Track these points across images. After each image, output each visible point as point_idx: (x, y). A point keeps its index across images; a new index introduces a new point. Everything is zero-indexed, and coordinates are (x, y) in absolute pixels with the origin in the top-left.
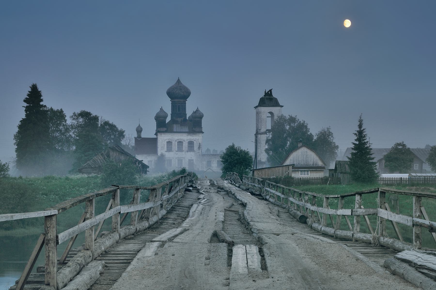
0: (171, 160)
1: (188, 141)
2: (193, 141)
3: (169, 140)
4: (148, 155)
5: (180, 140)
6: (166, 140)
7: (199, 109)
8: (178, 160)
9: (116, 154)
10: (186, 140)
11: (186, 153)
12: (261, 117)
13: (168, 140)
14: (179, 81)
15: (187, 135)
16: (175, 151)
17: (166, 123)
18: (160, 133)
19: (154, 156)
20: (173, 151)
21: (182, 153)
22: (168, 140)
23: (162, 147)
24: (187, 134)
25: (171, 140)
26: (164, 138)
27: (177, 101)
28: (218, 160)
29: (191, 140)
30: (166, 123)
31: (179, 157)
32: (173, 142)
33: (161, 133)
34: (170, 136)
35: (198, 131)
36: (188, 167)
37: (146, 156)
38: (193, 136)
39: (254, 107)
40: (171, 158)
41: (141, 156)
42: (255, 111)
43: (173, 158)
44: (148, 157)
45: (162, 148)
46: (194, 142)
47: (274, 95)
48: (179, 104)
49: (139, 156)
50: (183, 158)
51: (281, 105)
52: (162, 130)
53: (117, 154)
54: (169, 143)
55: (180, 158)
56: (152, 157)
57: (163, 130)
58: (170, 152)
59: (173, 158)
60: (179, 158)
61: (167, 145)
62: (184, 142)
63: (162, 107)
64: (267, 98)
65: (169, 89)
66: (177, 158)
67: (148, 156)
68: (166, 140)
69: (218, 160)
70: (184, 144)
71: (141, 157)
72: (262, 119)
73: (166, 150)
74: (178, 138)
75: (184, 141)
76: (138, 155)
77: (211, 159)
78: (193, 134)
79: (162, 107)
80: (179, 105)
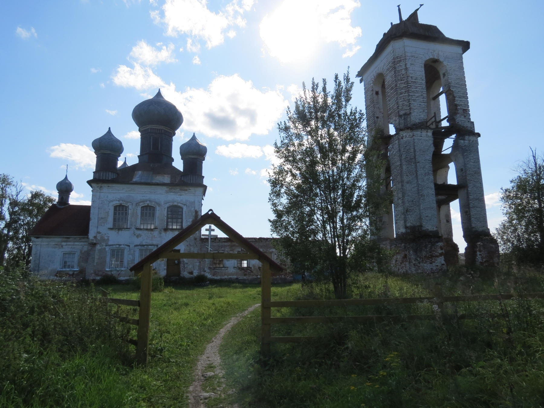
0: (123, 251)
1: (168, 205)
2: (179, 205)
3: (121, 202)
4: (65, 240)
5: (148, 202)
6: (112, 201)
8: (141, 250)
10: (162, 203)
11: (161, 233)
12: (403, 72)
13: (118, 202)
15: (167, 192)
16: (135, 229)
19: (81, 242)
20: (128, 227)
21: (152, 232)
22: (116, 203)
23: (102, 218)
24: (165, 188)
26: (107, 197)
27: (151, 128)
28: (240, 250)
29: (176, 204)
31: (144, 244)
32: (130, 207)
33: (100, 185)
35: (192, 182)
36: (166, 267)
37: (60, 240)
38: (181, 195)
40: (122, 246)
41: (45, 239)
43: (129, 246)
44: (64, 244)
46: (182, 208)
49: (40, 240)
50: (153, 247)
52: (104, 178)
55: (146, 247)
56: (76, 243)
58: (120, 231)
59: (129, 246)
60: (144, 246)
61: (115, 214)
62: (158, 208)
63: (110, 128)
66: (137, 246)
67: (64, 241)
68: (112, 201)
69: (240, 250)
70: (158, 213)
71: (47, 243)
72: (410, 78)
73: (111, 225)
74: (145, 198)
75: (159, 205)
76: (37, 238)
77: (223, 249)
78: (181, 190)
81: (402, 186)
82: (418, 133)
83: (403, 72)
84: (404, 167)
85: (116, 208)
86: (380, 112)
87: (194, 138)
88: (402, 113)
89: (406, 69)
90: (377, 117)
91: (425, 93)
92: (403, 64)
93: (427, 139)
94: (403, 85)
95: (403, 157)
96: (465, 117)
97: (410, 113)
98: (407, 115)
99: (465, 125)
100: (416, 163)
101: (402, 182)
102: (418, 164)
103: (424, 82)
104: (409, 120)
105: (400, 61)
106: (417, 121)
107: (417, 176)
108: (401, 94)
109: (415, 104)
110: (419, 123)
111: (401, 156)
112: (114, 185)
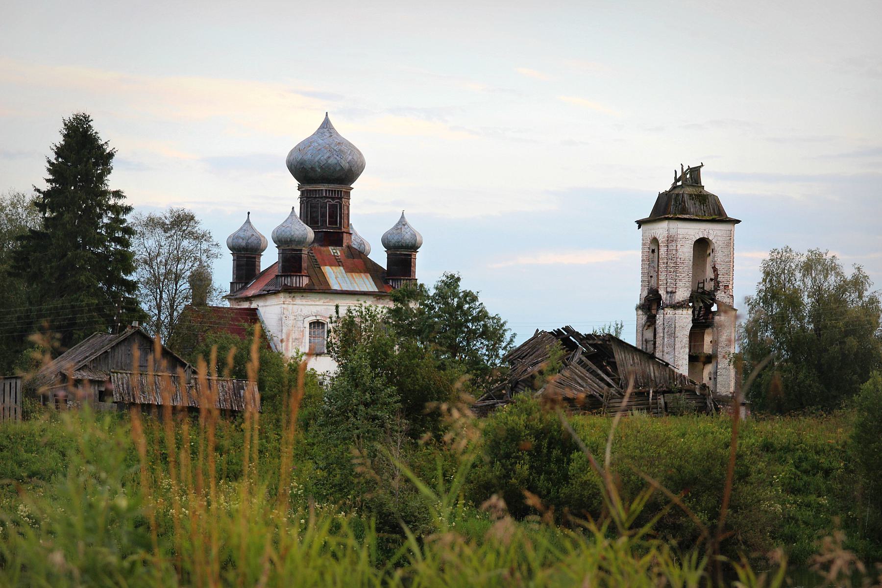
3: (318, 318)
7: (408, 219)
9: (633, 359)
12: (674, 252)
13: (314, 318)
14: (326, 124)
17: (384, 266)
18: (290, 293)
22: (313, 319)
23: (296, 339)
25: (323, 316)
26: (301, 311)
30: (384, 266)
33: (293, 295)
34: (321, 302)
39: (638, 222)
42: (638, 236)
45: (294, 344)
47: (709, 184)
48: (333, 199)
51: (730, 214)
53: (636, 361)
54: (314, 327)
57: (298, 285)
58: (318, 357)
63: (293, 208)
64: (691, 195)
65: (298, 149)
72: (679, 260)
79: (293, 208)
80: (333, 202)
81: (663, 355)
82: (679, 312)
83: (674, 252)
84: (666, 340)
85: (310, 324)
86: (655, 271)
87: (402, 222)
88: (669, 290)
89: (677, 250)
90: (651, 277)
91: (691, 272)
92: (674, 244)
93: (687, 316)
94: (672, 265)
95: (666, 330)
96: (725, 293)
97: (675, 292)
98: (672, 292)
99: (724, 301)
100: (674, 337)
101: (663, 352)
102: (676, 339)
103: (691, 263)
104: (673, 297)
105: (673, 241)
106: (681, 299)
107: (674, 349)
108: (670, 272)
109: (680, 284)
110: (683, 301)
111: (664, 329)
112: (313, 295)
